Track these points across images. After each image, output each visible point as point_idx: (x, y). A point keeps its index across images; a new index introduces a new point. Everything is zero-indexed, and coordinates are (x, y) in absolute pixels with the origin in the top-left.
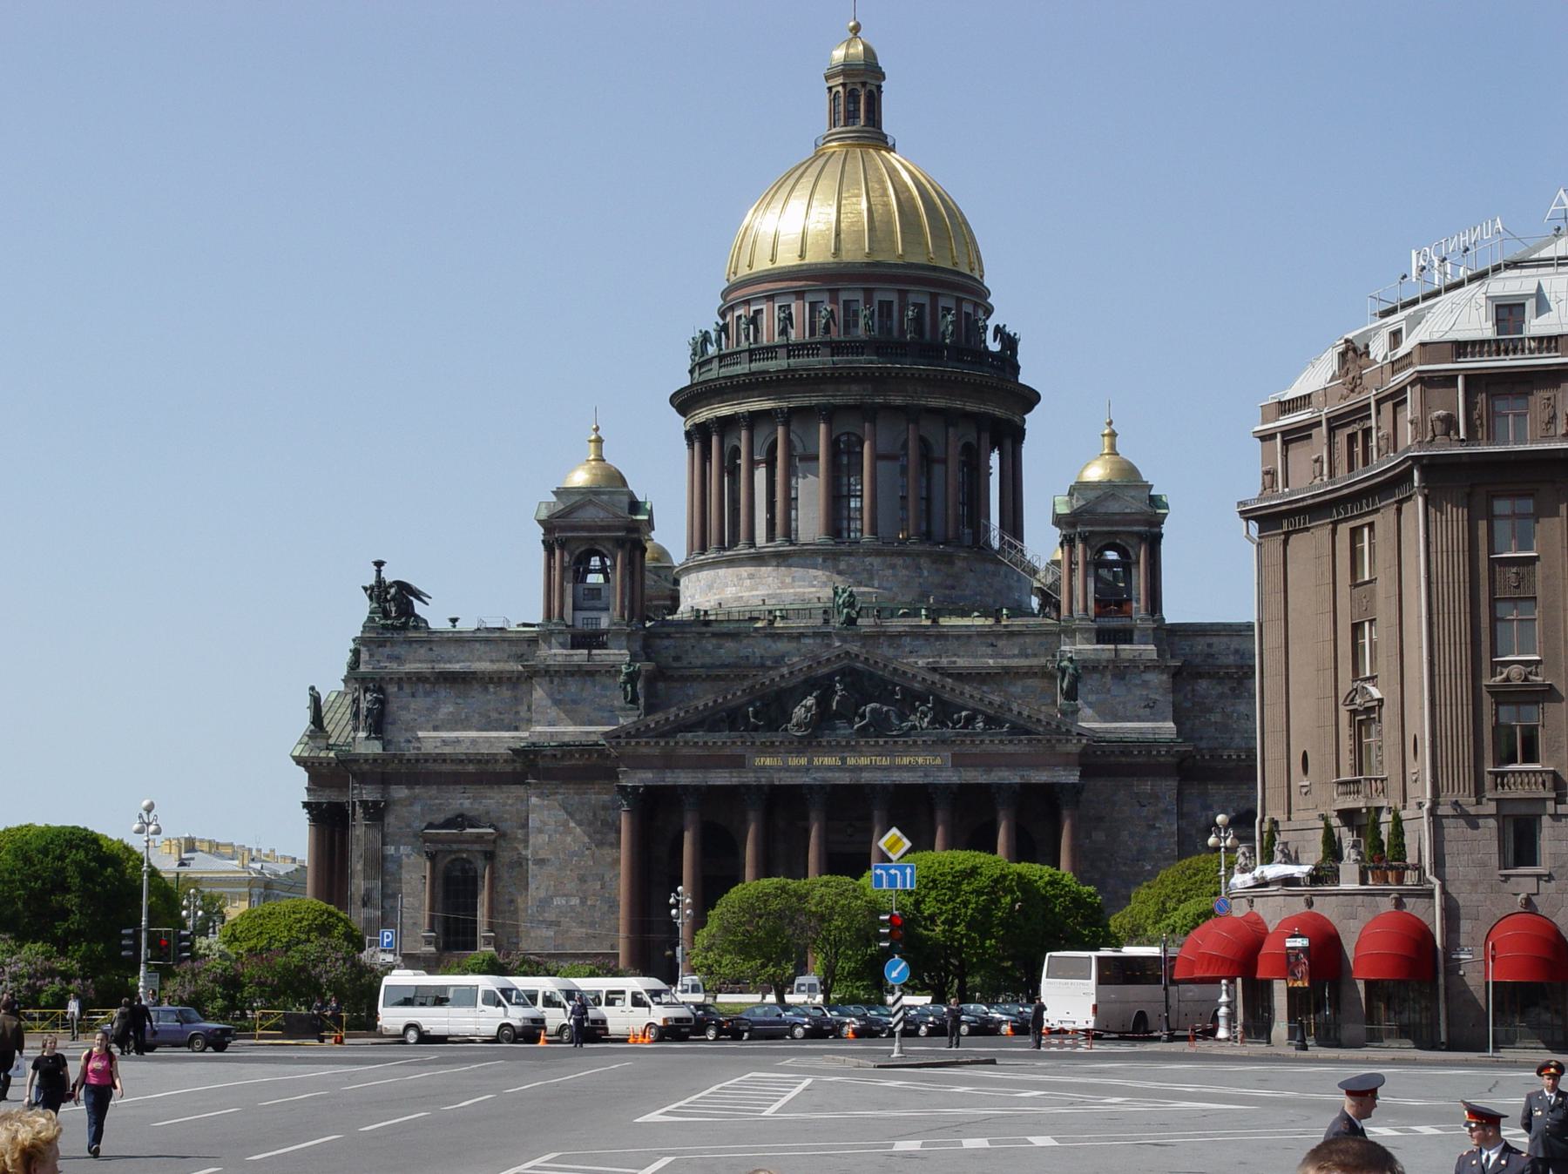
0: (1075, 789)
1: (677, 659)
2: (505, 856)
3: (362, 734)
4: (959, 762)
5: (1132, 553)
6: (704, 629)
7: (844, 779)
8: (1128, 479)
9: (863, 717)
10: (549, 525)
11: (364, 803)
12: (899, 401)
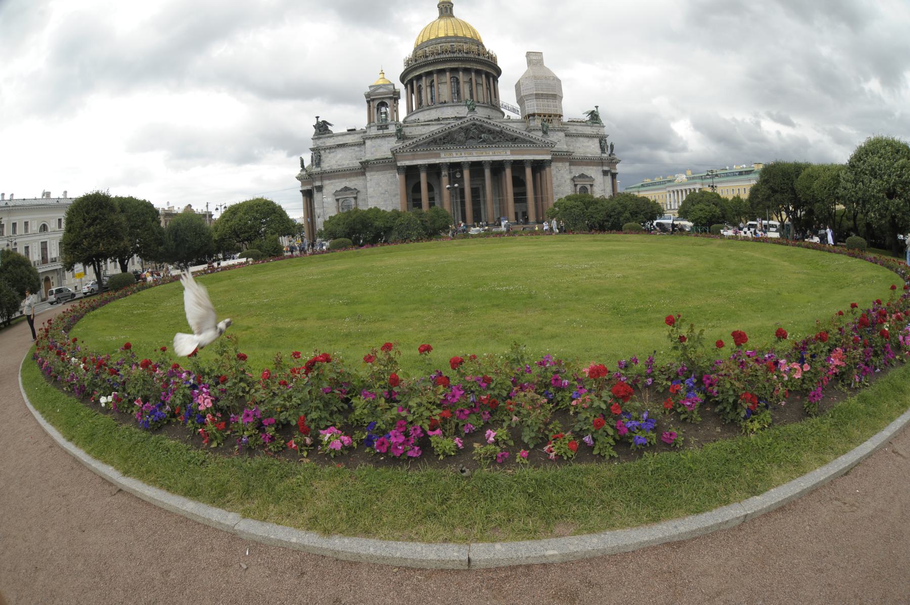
0: (549, 162)
2: (360, 197)
11: (316, 187)
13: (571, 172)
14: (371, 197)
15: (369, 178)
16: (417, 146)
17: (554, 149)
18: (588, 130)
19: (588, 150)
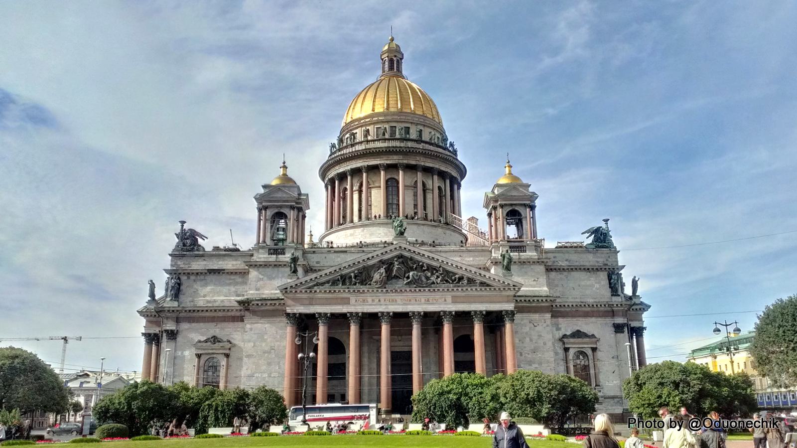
1: (318, 263)
3: (168, 299)
4: (455, 300)
5: (523, 214)
6: (331, 249)
7: (400, 309)
8: (516, 184)
9: (408, 278)
10: (259, 199)
11: (166, 331)
12: (413, 163)
13: (558, 329)
14: (249, 356)
15: (248, 326)
16: (317, 285)
17: (519, 294)
18: (590, 260)
19: (588, 292)
